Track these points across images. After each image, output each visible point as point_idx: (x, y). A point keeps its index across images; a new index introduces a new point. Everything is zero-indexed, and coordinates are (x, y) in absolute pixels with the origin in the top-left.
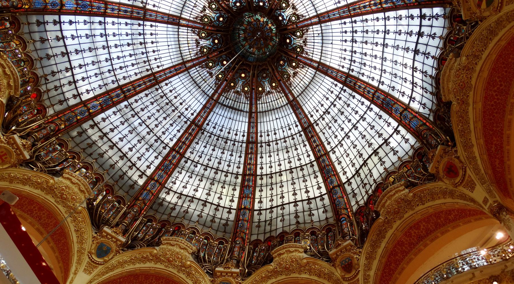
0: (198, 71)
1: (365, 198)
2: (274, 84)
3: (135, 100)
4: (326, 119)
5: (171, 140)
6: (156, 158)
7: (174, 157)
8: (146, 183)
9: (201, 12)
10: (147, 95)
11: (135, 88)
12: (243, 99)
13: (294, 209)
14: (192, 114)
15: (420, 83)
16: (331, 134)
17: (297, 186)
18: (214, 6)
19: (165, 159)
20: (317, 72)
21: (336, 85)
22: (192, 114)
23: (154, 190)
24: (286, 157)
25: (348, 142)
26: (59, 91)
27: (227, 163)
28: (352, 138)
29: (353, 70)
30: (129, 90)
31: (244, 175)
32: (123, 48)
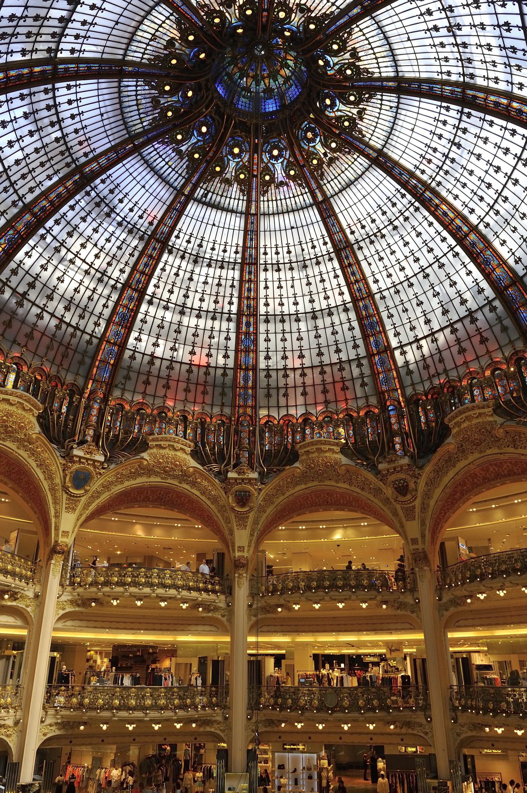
0: (268, 201)
2: (352, 98)
3: (265, 305)
5: (341, 294)
7: (366, 307)
8: (372, 366)
10: (266, 287)
11: (248, 298)
14: (325, 244)
18: (179, 137)
20: (374, 15)
22: (325, 244)
27: (425, 250)
30: (249, 307)
31: (460, 241)
32: (193, 289)
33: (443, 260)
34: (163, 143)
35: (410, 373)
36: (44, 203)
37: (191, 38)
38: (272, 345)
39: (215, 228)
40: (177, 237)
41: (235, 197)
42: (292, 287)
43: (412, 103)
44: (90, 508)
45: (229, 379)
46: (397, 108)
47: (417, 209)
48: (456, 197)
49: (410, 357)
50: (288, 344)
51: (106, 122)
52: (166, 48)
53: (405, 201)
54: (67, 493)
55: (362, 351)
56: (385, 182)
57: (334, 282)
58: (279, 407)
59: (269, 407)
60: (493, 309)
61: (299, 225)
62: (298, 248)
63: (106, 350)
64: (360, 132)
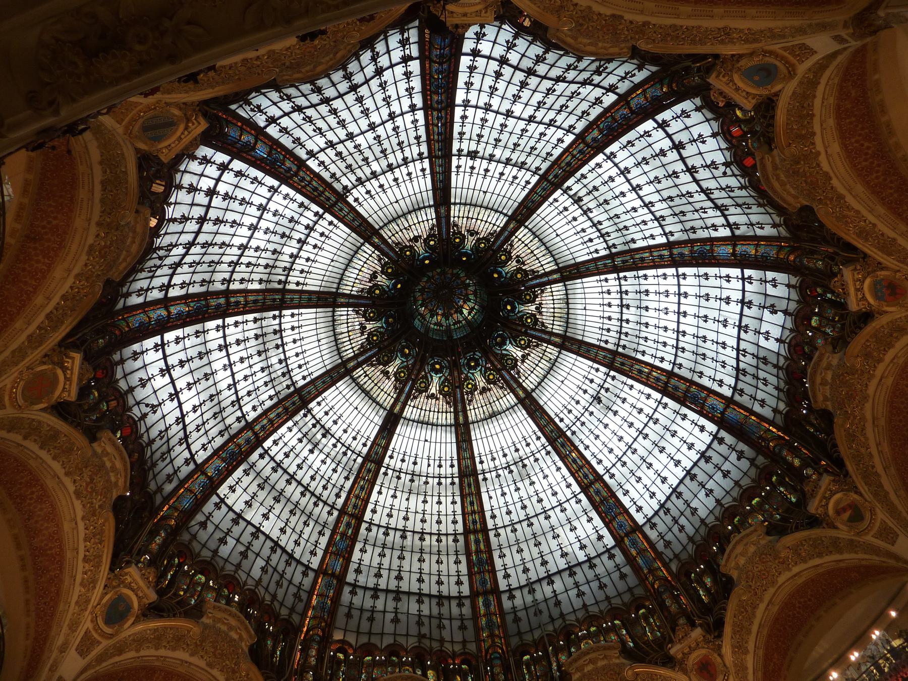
1: (782, 395)
4: (630, 332)
6: (457, 562)
9: (362, 334)
10: (380, 493)
12: (496, 391)
13: (695, 483)
15: (728, 202)
16: (655, 346)
17: (670, 449)
19: (468, 554)
21: (606, 280)
23: (492, 607)
24: (620, 422)
25: (688, 338)
26: (285, 583)
28: (691, 330)
29: (614, 246)
31: (585, 489)
33: (566, 505)
34: (357, 313)
35: (517, 620)
36: (242, 299)
37: (432, 243)
38: (366, 557)
39: (356, 412)
40: (319, 404)
41: (386, 391)
42: (408, 499)
43: (569, 358)
44: (104, 664)
45: (307, 582)
46: (556, 360)
47: (548, 453)
48: (587, 447)
49: (518, 602)
50: (386, 562)
51: (330, 268)
52: (411, 240)
53: (538, 444)
54: (92, 621)
55: (466, 590)
56: (525, 422)
57: (450, 508)
58: (358, 633)
59: (345, 630)
60: (612, 557)
61: (433, 440)
62: (425, 462)
63: (198, 481)
64: (518, 373)
